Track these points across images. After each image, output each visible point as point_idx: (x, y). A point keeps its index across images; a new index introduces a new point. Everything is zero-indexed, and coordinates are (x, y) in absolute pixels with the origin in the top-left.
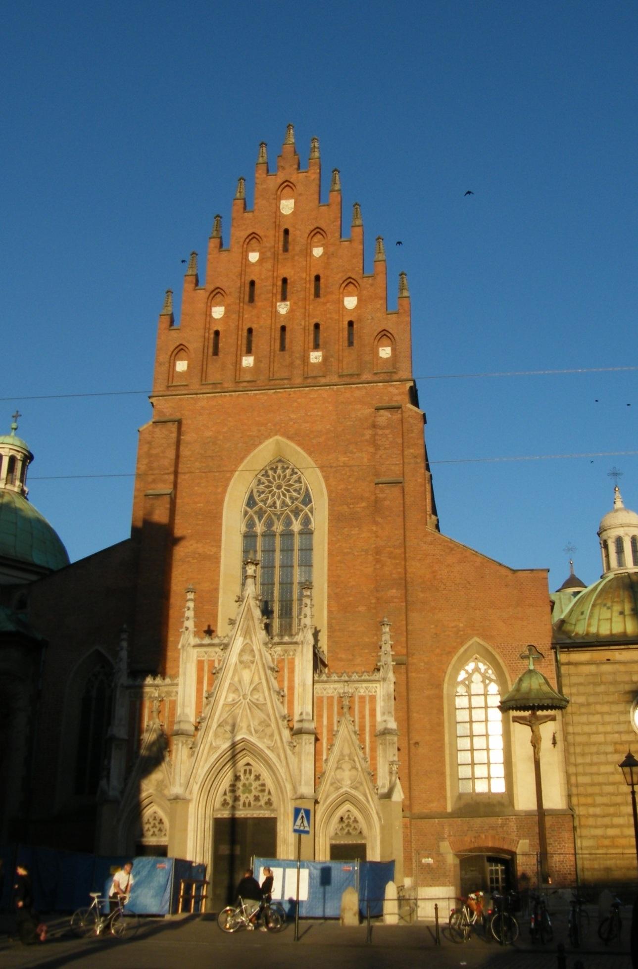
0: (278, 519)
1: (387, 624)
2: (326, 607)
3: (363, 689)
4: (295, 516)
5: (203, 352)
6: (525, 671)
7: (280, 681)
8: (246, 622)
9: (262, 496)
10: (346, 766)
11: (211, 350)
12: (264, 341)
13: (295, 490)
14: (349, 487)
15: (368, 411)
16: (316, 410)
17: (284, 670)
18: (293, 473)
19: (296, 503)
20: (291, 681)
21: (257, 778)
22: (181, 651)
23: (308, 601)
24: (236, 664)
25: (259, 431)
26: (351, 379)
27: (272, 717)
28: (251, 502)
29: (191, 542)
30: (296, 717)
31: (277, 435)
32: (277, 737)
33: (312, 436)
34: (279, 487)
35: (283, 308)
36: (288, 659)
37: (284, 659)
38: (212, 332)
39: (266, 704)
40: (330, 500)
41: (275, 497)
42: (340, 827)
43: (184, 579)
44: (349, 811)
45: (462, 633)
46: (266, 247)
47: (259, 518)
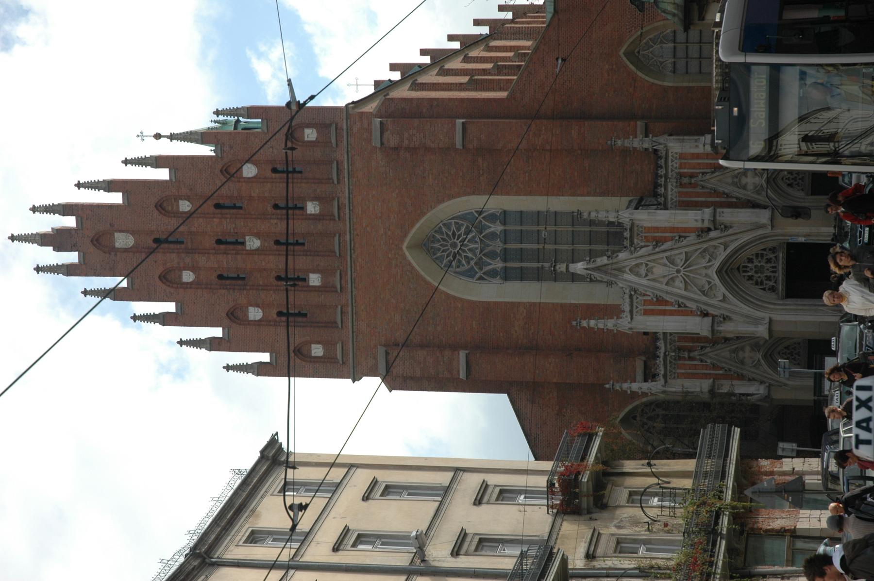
0: (488, 247)
1: (615, 141)
2: (583, 198)
3: (674, 165)
4: (485, 229)
5: (304, 326)
6: (655, 7)
9: (464, 262)
10: (744, 180)
11: (300, 319)
13: (459, 230)
14: (461, 174)
16: (376, 207)
17: (656, 236)
18: (439, 231)
20: (665, 230)
21: (750, 261)
22: (635, 331)
23: (593, 215)
24: (648, 280)
27: (698, 246)
28: (470, 274)
30: (699, 225)
32: (715, 243)
33: (405, 211)
34: (454, 245)
36: (645, 232)
37: (645, 236)
38: (278, 319)
39: (686, 252)
40: (473, 194)
41: (466, 249)
42: (796, 186)
44: (782, 179)
45: (614, 67)
46: (178, 263)
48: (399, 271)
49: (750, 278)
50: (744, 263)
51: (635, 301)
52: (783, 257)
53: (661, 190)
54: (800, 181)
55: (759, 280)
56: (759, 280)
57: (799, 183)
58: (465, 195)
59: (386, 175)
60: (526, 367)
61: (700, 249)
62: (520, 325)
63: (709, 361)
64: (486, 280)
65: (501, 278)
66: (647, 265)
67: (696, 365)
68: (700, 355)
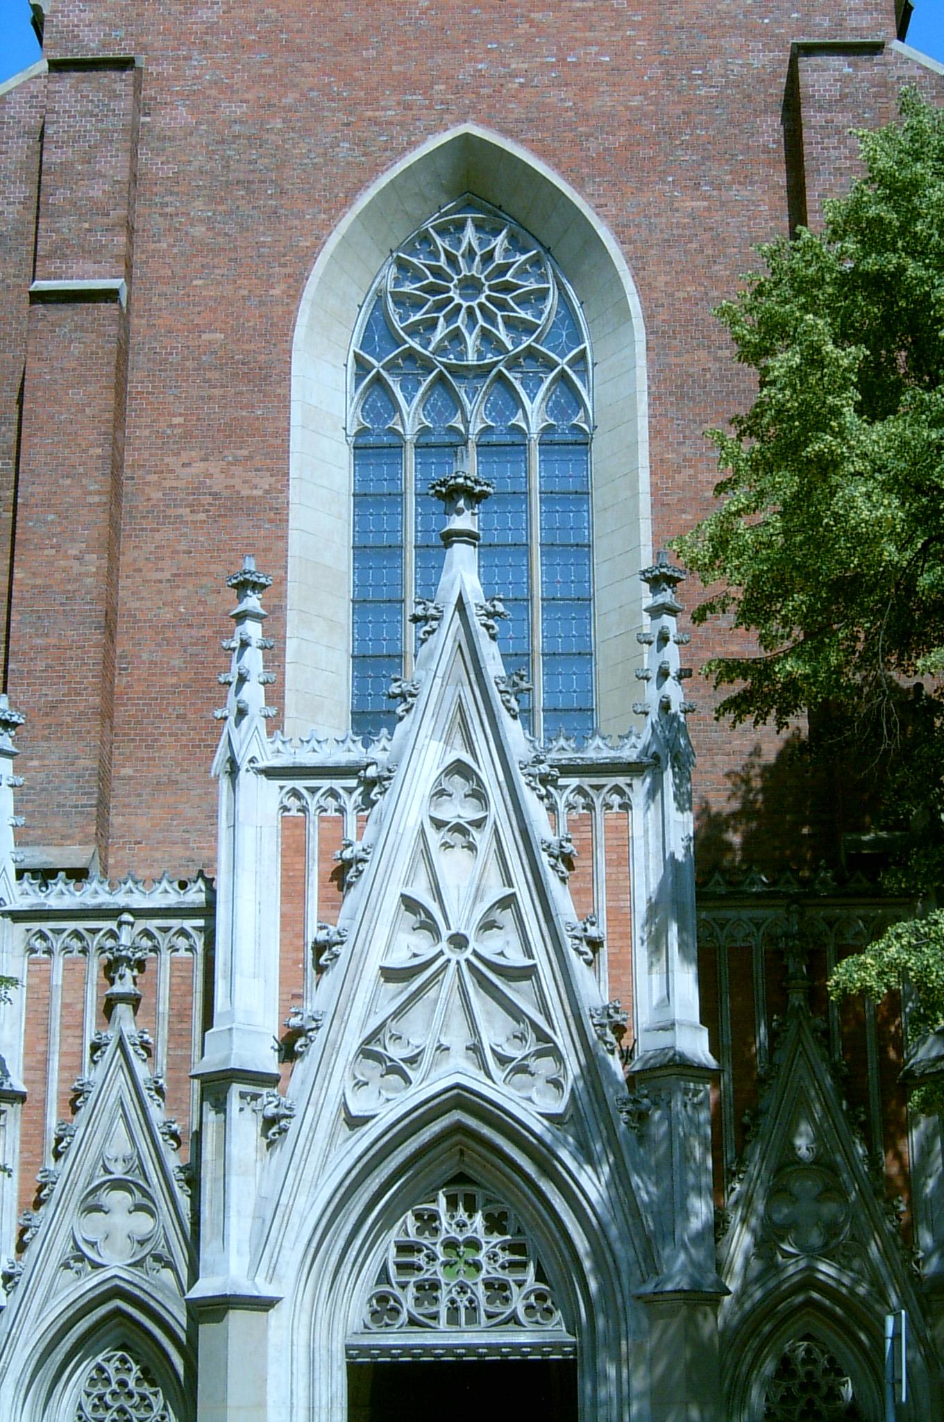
8: (450, 691)
14: (715, 294)
16: (594, 49)
19: (527, 341)
24: (423, 832)
25: (408, 107)
29: (185, 456)
30: (644, 1016)
31: (465, 122)
34: (470, 286)
43: (167, 575)
47: (403, 388)
48: (389, 113)
50: (488, 1201)
51: (337, 784)
52: (516, 1347)
54: (801, 1405)
55: (420, 1259)
56: (420, 1259)
57: (795, 1400)
58: (644, 309)
59: (700, 77)
60: (68, 482)
61: (553, 1028)
62: (211, 476)
63: (92, 1075)
64: (356, 388)
65: (362, 432)
66: (479, 824)
67: (82, 1026)
68: (121, 1039)
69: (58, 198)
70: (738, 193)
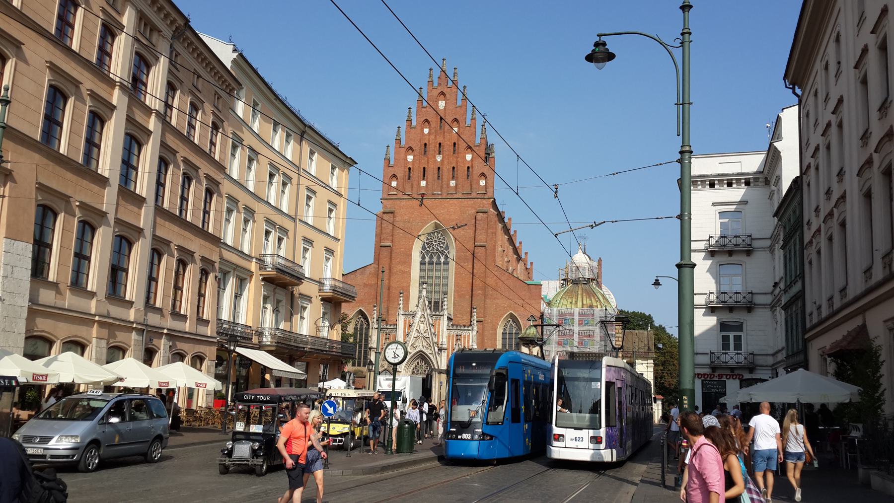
7: (435, 329)
11: (407, 177)
12: (431, 173)
13: (442, 243)
15: (474, 211)
20: (439, 329)
26: (467, 196)
28: (424, 248)
30: (440, 343)
32: (433, 350)
34: (436, 241)
35: (439, 158)
49: (418, 363)
53: (455, 328)
69: (383, 232)
70: (468, 231)
